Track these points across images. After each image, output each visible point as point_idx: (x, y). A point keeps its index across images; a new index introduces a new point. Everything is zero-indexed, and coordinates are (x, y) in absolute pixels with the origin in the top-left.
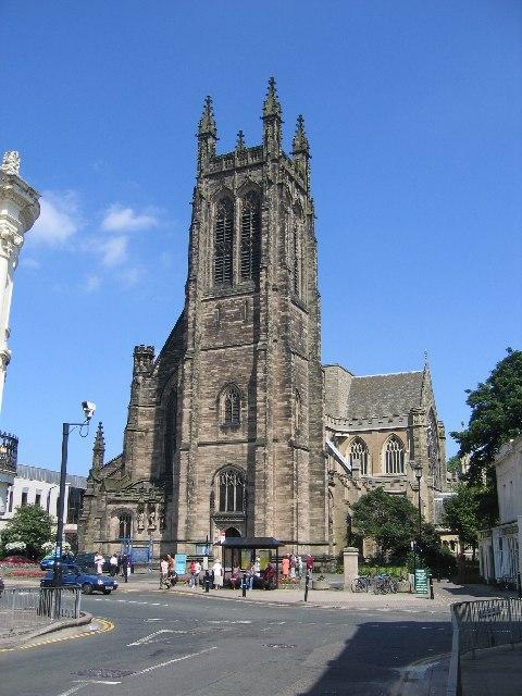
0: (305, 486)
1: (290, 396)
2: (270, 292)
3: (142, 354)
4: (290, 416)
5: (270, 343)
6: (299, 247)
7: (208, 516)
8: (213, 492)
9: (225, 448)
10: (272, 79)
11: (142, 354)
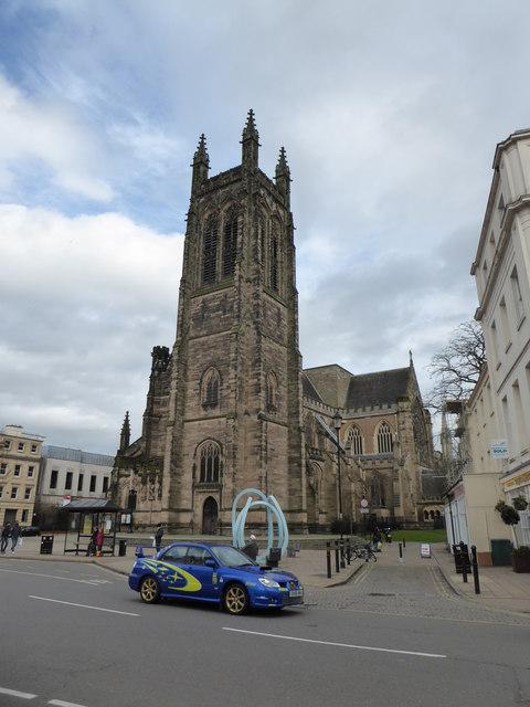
0: (284, 458)
1: (260, 374)
5: (243, 327)
10: (251, 110)
11: (160, 354)
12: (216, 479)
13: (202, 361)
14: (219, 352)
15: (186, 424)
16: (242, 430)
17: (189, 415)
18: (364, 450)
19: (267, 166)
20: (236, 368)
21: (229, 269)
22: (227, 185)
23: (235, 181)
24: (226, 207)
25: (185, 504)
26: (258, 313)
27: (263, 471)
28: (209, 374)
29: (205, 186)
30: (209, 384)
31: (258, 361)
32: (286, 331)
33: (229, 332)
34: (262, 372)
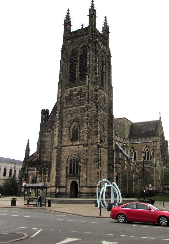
0: (106, 164)
1: (98, 126)
2: (90, 85)
3: (45, 112)
4: (98, 134)
6: (104, 68)
7: (65, 176)
8: (67, 166)
9: (72, 148)
11: (45, 112)
12: (77, 173)
13: (70, 119)
14: (79, 115)
15: (63, 148)
16: (90, 152)
17: (64, 144)
18: (137, 158)
19: (99, 27)
20: (87, 124)
21: (83, 77)
22: (81, 36)
23: (86, 34)
24: (81, 46)
25: (63, 184)
26: (97, 98)
27: (99, 170)
28: (73, 125)
29: (70, 37)
30: (73, 130)
31: (97, 120)
32: (107, 105)
33: (84, 106)
34: (99, 125)
